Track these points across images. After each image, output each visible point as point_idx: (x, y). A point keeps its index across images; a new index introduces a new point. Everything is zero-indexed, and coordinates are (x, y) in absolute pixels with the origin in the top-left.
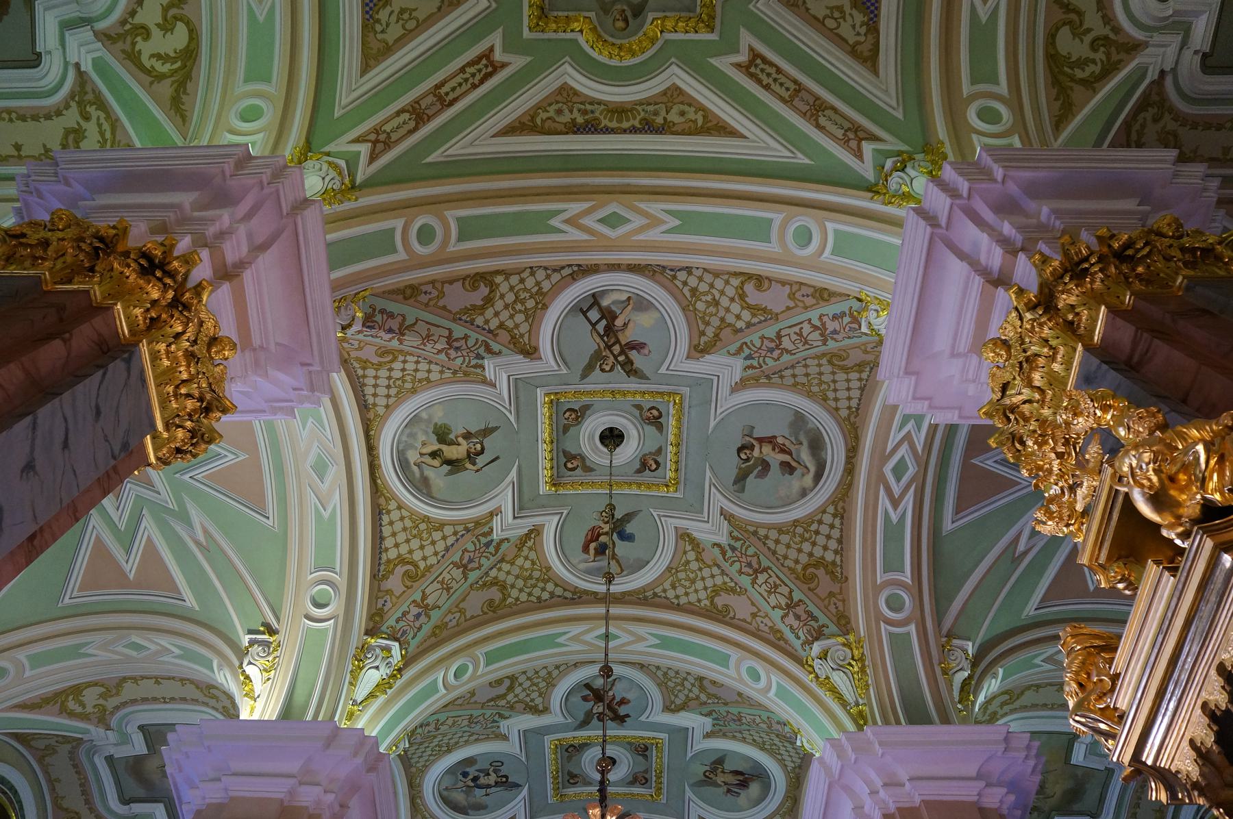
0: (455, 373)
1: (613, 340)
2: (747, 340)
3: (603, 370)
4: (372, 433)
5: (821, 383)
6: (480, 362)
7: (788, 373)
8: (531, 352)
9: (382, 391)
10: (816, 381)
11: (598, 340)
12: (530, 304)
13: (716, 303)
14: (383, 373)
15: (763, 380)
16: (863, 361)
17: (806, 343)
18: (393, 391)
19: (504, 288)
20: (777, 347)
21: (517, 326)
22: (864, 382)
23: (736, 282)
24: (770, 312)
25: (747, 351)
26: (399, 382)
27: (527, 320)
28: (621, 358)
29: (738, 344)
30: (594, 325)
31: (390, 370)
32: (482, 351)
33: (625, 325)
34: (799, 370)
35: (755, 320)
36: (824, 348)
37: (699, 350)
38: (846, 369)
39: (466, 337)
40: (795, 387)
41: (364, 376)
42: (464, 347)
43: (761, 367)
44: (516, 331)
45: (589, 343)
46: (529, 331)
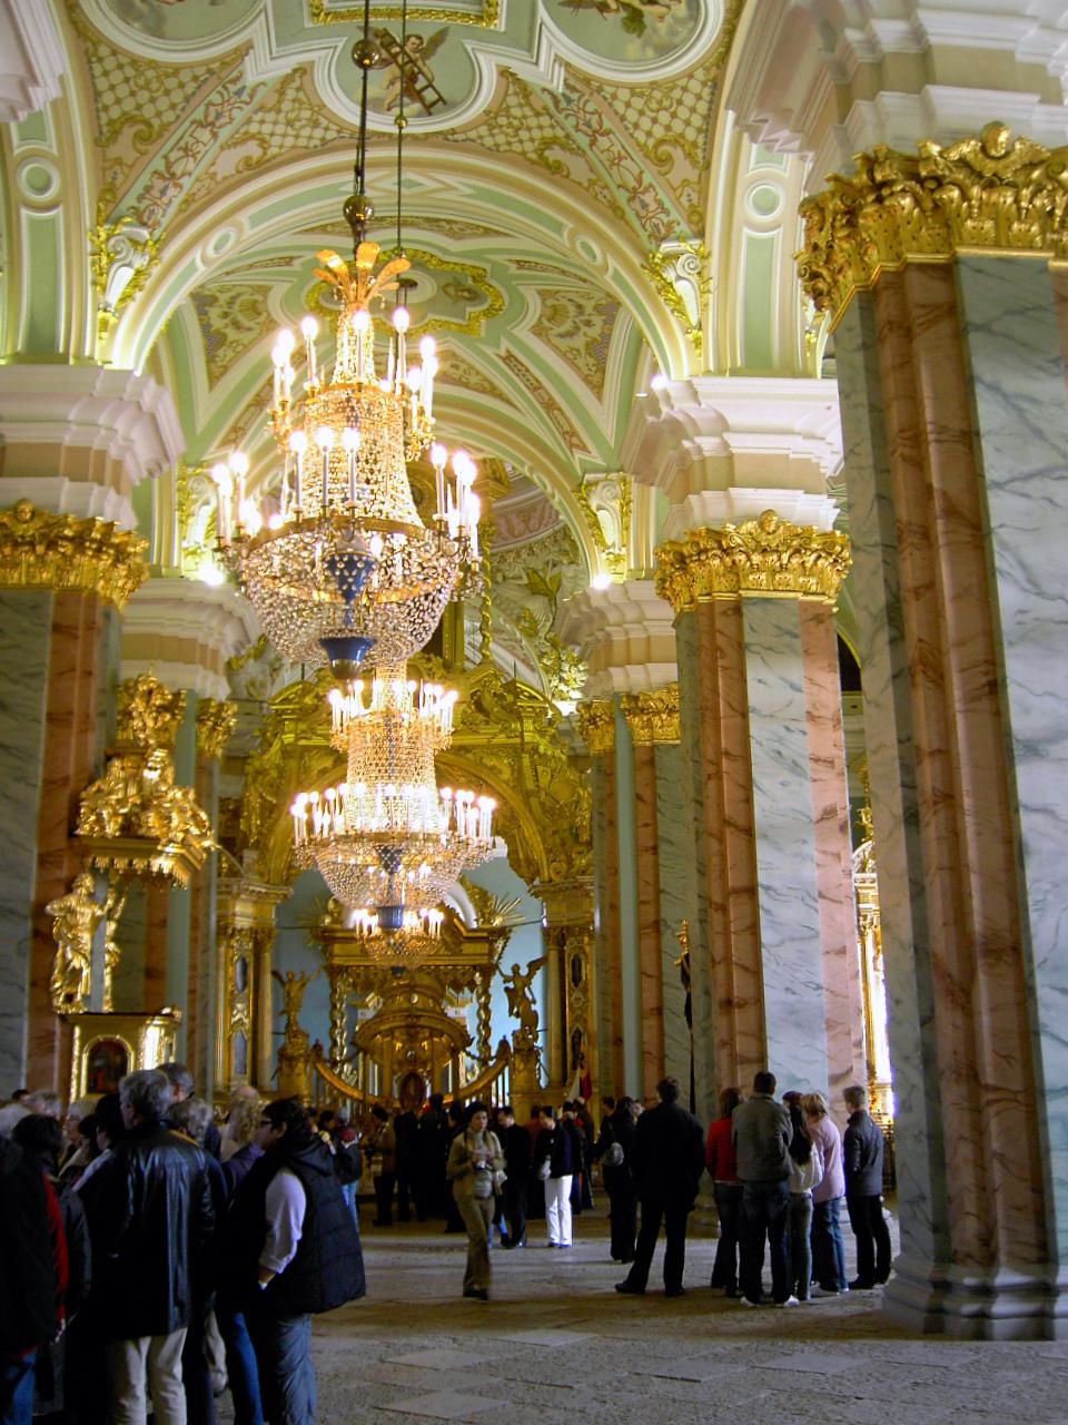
0: (599, 90)
1: (408, 67)
2: (247, 109)
3: (419, 38)
4: (721, 49)
5: (147, 86)
6: (568, 93)
7: (190, 88)
8: (505, 73)
9: (689, 100)
10: (154, 86)
11: (425, 69)
12: (502, 121)
13: (289, 123)
14: (678, 126)
15: (215, 66)
16: (115, 141)
17: (185, 150)
18: (677, 94)
19: (529, 147)
20: (212, 124)
21: (521, 106)
22: (100, 105)
23: (274, 151)
24: (229, 147)
25: (245, 97)
26: (666, 103)
27: (508, 108)
28: (396, 50)
29: (257, 98)
30: (430, 85)
31: (668, 128)
32: (563, 104)
33: (392, 83)
34: (177, 97)
35: (242, 131)
36: (163, 152)
37: (303, 71)
38: (128, 119)
39: (577, 128)
40: (176, 70)
41: (699, 130)
42: (581, 122)
43: (224, 87)
44: (522, 101)
45: (434, 66)
46: (506, 95)
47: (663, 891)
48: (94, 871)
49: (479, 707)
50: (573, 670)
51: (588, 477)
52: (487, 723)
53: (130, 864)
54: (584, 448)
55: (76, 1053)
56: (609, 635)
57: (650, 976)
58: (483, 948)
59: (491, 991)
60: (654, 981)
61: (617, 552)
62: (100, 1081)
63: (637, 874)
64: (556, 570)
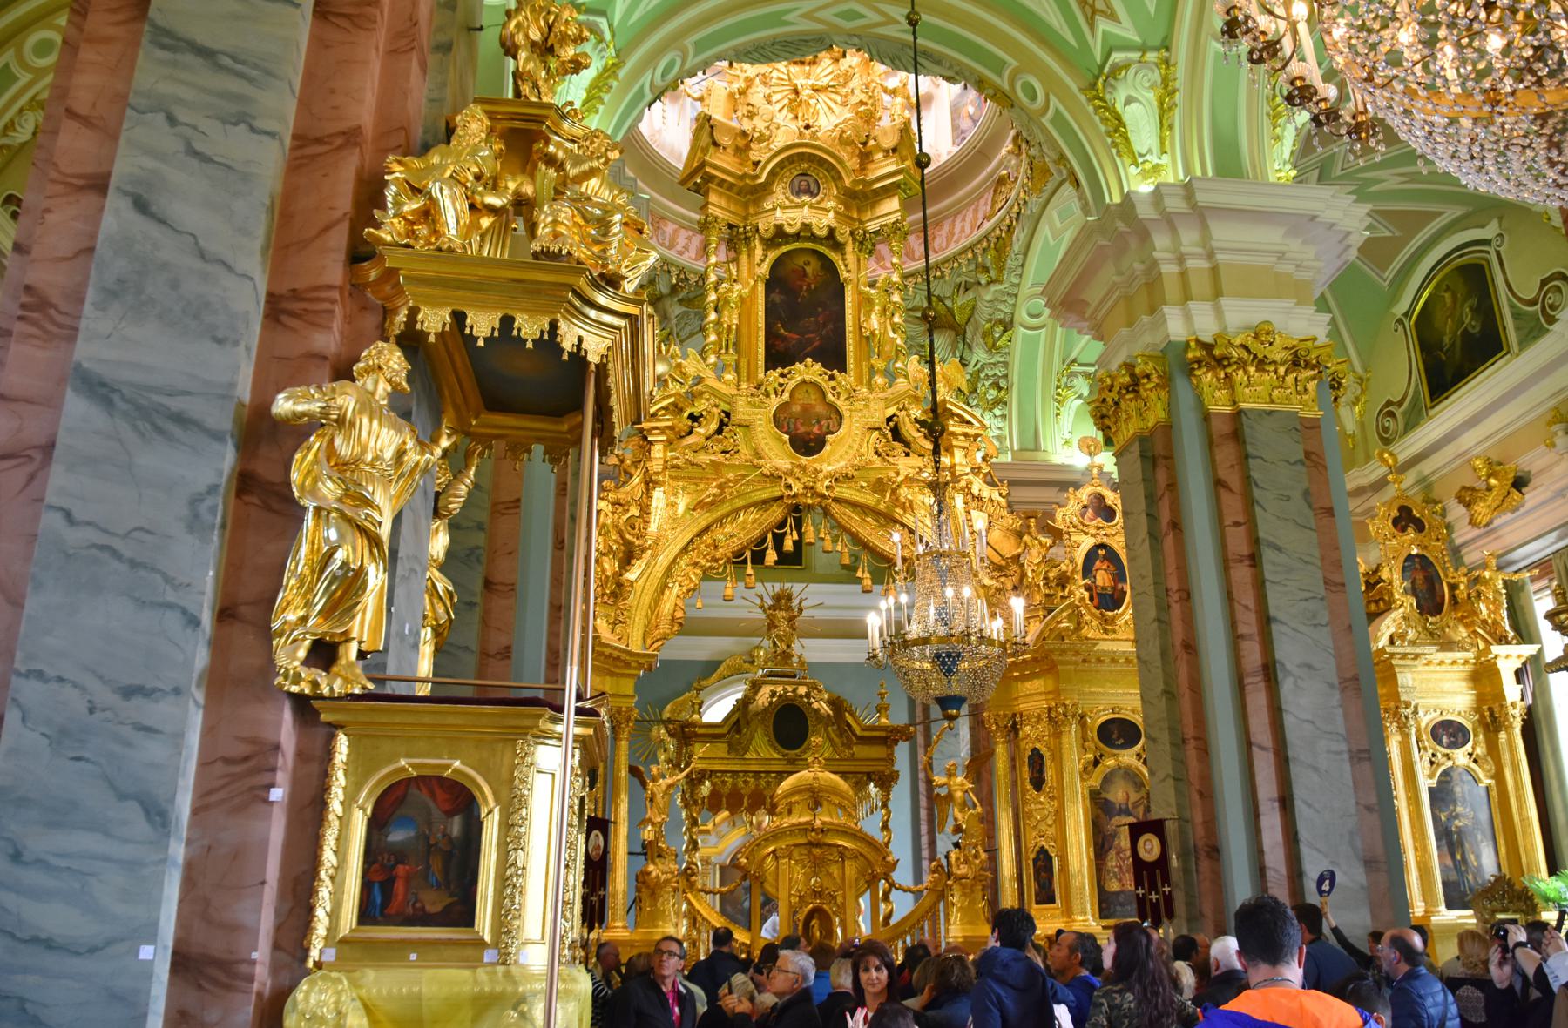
47: (1275, 620)
48: (411, 342)
49: (897, 434)
50: (988, 415)
51: (1117, 57)
52: (907, 455)
53: (507, 322)
54: (1112, 16)
55: (336, 806)
56: (1155, 264)
57: (1262, 748)
58: (877, 752)
59: (890, 805)
60: (1271, 756)
61: (1156, 161)
62: (399, 887)
63: (1229, 596)
64: (970, 295)
